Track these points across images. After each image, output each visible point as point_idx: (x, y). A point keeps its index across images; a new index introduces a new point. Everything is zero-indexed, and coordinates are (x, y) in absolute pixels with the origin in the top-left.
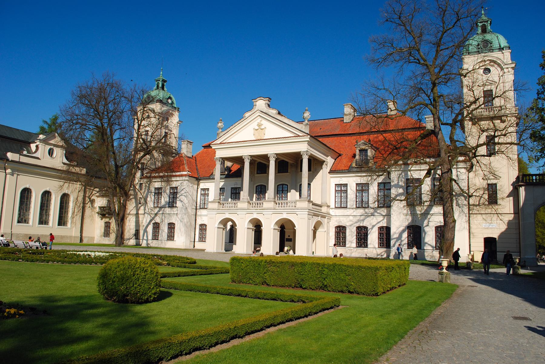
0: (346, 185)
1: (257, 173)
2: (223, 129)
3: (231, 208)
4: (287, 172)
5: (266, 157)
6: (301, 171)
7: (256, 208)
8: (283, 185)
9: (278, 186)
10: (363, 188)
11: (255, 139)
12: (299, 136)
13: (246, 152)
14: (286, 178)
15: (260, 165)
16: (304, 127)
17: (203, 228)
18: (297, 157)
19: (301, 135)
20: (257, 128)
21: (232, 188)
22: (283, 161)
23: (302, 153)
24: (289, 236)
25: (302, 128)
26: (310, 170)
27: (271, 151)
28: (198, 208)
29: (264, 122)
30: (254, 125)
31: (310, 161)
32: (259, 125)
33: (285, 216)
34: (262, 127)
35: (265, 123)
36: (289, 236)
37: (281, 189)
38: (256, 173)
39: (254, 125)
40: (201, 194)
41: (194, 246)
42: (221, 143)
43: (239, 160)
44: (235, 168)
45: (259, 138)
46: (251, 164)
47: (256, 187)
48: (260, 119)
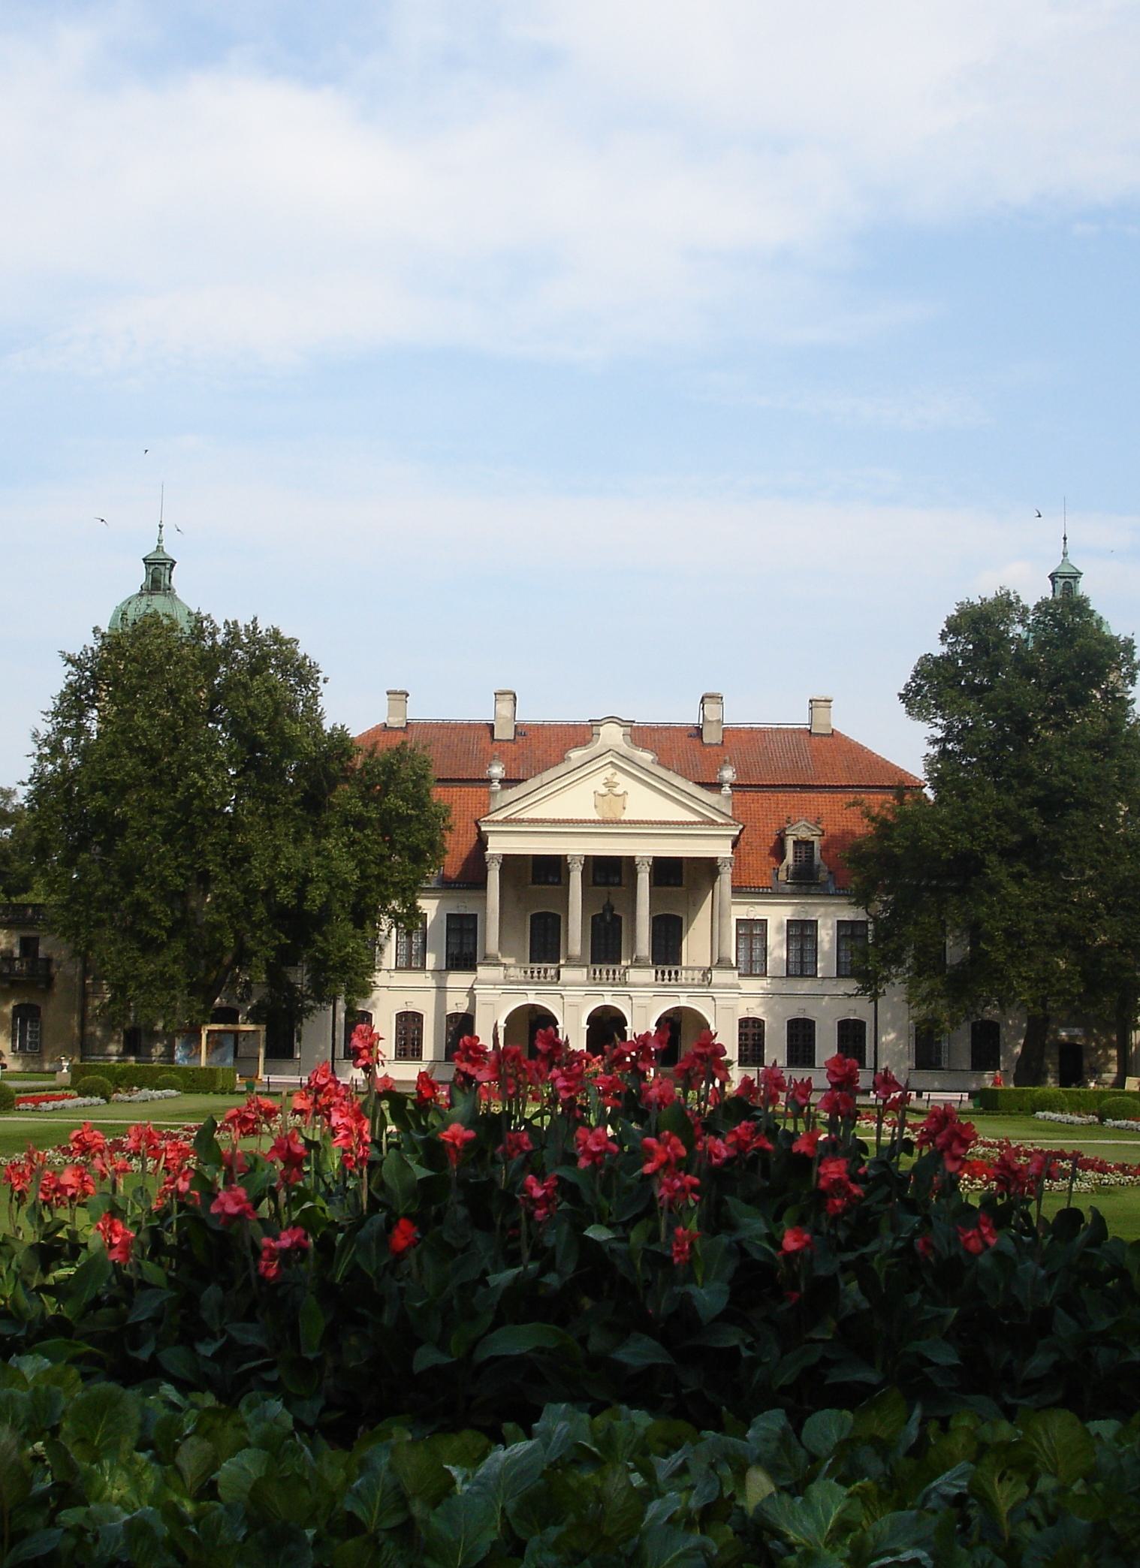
0: (763, 923)
1: (534, 883)
2: (508, 782)
10: (801, 932)
11: (597, 817)
12: (713, 823)
13: (576, 848)
16: (723, 802)
19: (720, 820)
20: (604, 790)
25: (718, 803)
27: (645, 849)
29: (620, 777)
30: (597, 783)
32: (610, 784)
33: (683, 1002)
34: (618, 790)
35: (624, 783)
39: (597, 783)
42: (507, 821)
45: (610, 816)
48: (612, 770)
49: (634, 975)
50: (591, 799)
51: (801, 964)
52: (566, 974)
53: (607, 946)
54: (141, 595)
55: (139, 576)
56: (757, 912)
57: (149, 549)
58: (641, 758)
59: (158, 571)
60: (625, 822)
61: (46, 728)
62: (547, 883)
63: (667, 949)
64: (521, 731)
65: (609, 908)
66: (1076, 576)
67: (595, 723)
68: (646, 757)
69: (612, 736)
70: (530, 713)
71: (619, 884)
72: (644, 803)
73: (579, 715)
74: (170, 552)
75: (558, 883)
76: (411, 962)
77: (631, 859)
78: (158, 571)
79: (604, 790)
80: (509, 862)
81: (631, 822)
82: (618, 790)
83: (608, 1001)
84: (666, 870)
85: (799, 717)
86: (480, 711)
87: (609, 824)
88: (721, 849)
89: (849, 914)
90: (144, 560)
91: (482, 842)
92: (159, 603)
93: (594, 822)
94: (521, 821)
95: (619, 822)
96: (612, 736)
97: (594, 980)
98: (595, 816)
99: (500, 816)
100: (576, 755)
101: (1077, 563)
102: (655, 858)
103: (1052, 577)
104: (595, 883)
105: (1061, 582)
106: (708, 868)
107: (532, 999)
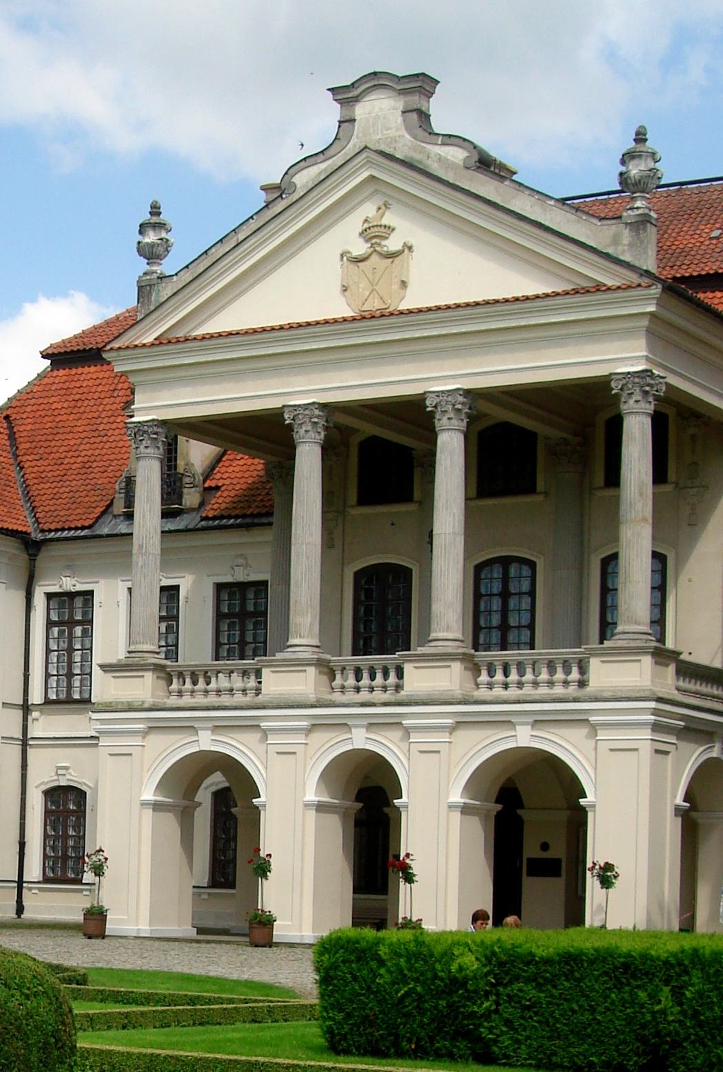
3: (225, 700)
4: (531, 489)
5: (413, 415)
6: (613, 477)
7: (364, 696)
8: (505, 562)
9: (479, 569)
11: (349, 313)
12: (599, 288)
14: (527, 527)
15: (380, 455)
16: (626, 235)
17: (67, 806)
18: (585, 413)
19: (610, 283)
20: (360, 248)
21: (220, 587)
22: (505, 427)
23: (615, 386)
24: (545, 847)
25: (616, 241)
26: (660, 476)
28: (36, 697)
30: (346, 235)
31: (659, 423)
32: (374, 233)
34: (393, 244)
36: (545, 847)
37: (496, 587)
38: (353, 496)
39: (346, 235)
40: (50, 624)
41: (20, 909)
42: (159, 342)
43: (266, 434)
44: (244, 469)
45: (374, 305)
46: (329, 450)
47: (358, 575)
50: (334, 271)
58: (440, 159)
60: (401, 313)
75: (406, 497)
79: (360, 248)
82: (393, 244)
99: (149, 339)
102: (468, 393)
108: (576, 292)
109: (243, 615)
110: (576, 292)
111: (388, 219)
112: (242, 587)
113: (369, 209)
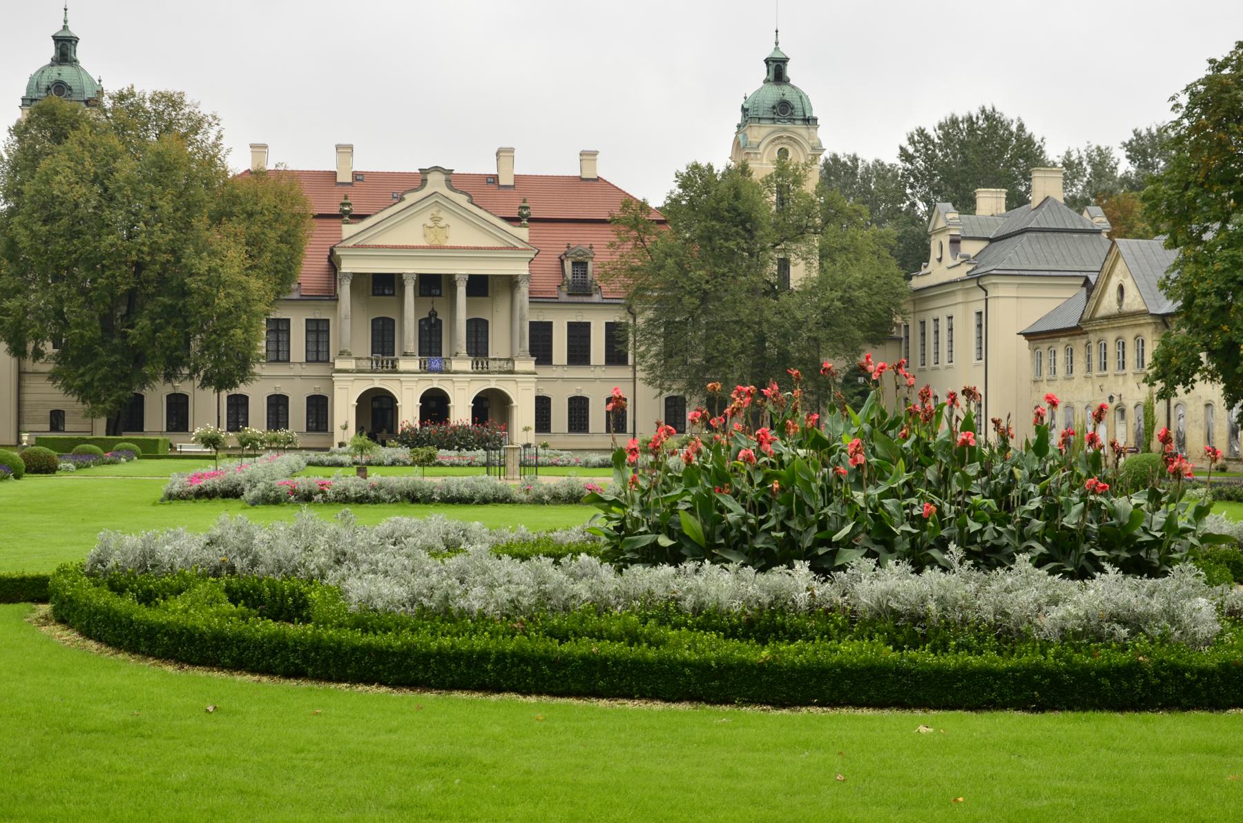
10: (579, 334)
11: (425, 244)
12: (515, 248)
13: (410, 268)
27: (462, 269)
30: (426, 219)
32: (435, 219)
33: (493, 385)
34: (442, 224)
35: (446, 218)
39: (426, 219)
42: (356, 246)
45: (436, 243)
49: (456, 365)
51: (579, 355)
52: (403, 365)
53: (431, 342)
54: (52, 65)
55: (50, 51)
56: (545, 317)
57: (57, 28)
59: (65, 46)
60: (448, 248)
61: (943, 121)
62: (384, 294)
63: (478, 344)
64: (357, 176)
65: (433, 314)
66: (784, 61)
67: (424, 172)
68: (462, 199)
69: (436, 183)
70: (363, 162)
71: (440, 295)
72: (460, 234)
73: (412, 166)
74: (74, 30)
76: (280, 355)
77: (450, 280)
78: (65, 46)
79: (430, 224)
80: (357, 278)
81: (451, 248)
82: (442, 224)
83: (435, 385)
84: (478, 286)
85: (572, 169)
86: (328, 163)
87: (436, 249)
88: (521, 269)
89: (616, 316)
90: (54, 37)
91: (333, 263)
92: (66, 73)
93: (423, 247)
94: (369, 247)
95: (444, 248)
96: (436, 183)
97: (426, 369)
98: (424, 243)
99: (351, 244)
100: (410, 198)
101: (786, 50)
102: (470, 276)
103: (767, 61)
104: (421, 295)
105: (773, 66)
106: (511, 282)
107: (377, 384)
108: (507, 248)
109: (318, 332)
110: (507, 248)
111: (441, 215)
112: (317, 321)
113: (434, 211)
